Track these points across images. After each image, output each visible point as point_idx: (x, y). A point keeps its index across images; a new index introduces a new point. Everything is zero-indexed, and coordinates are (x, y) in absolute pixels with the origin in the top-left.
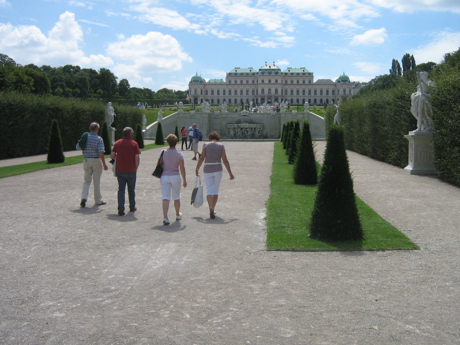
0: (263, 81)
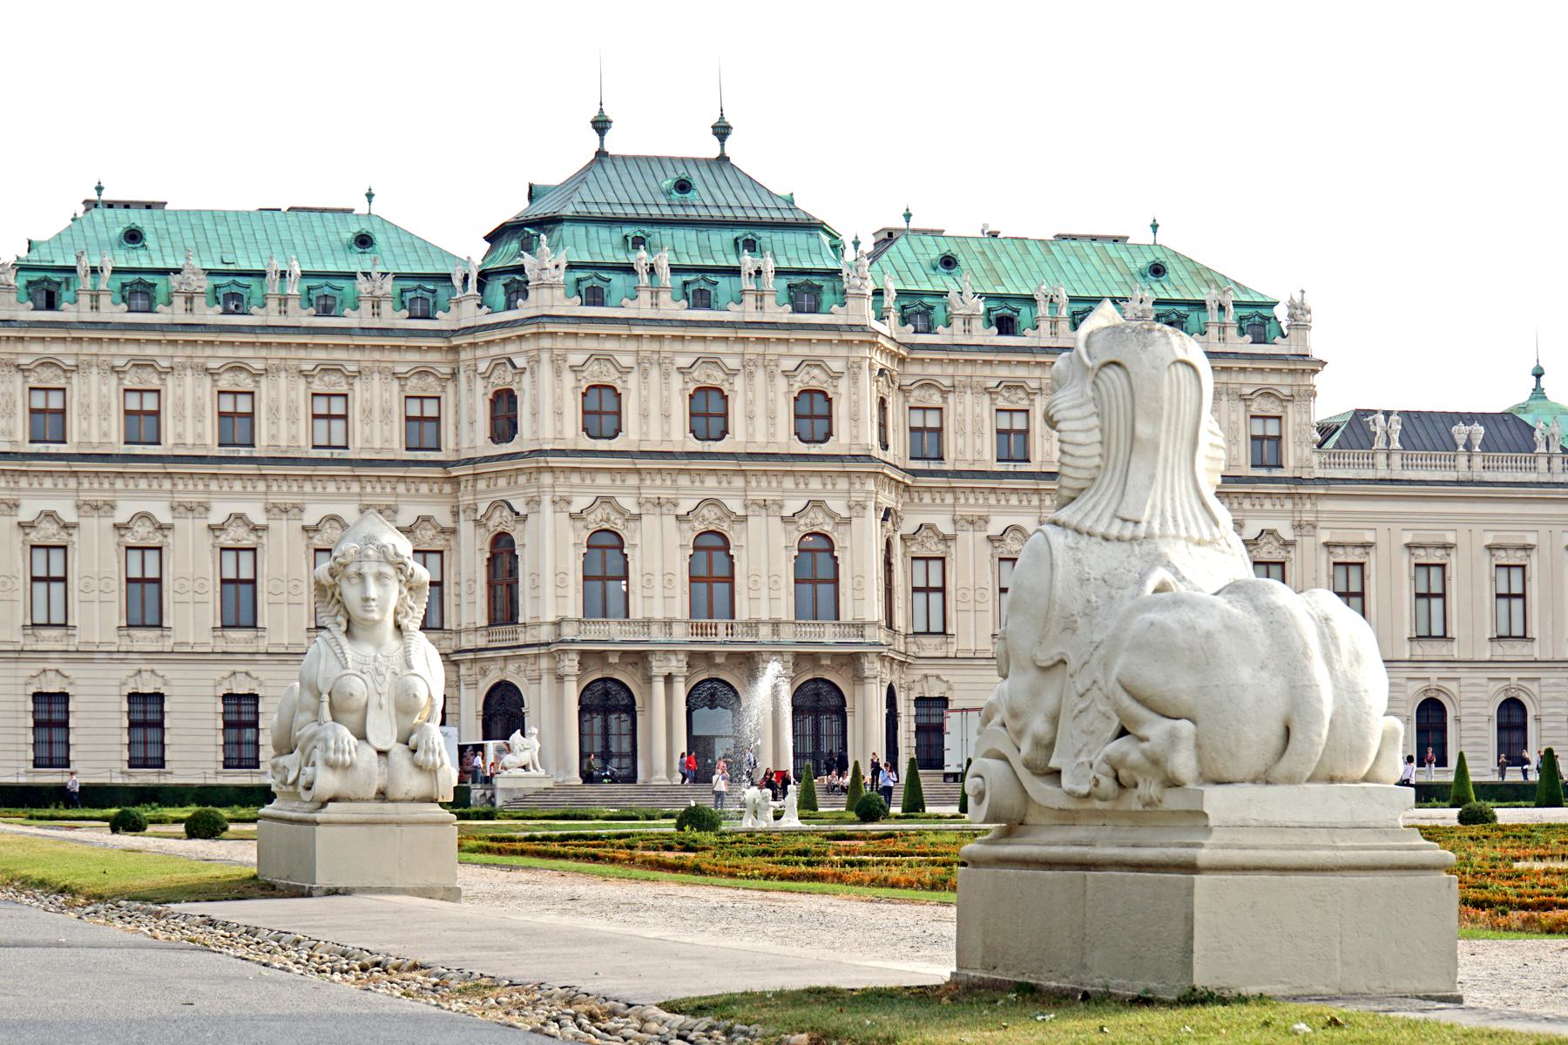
0: (602, 409)
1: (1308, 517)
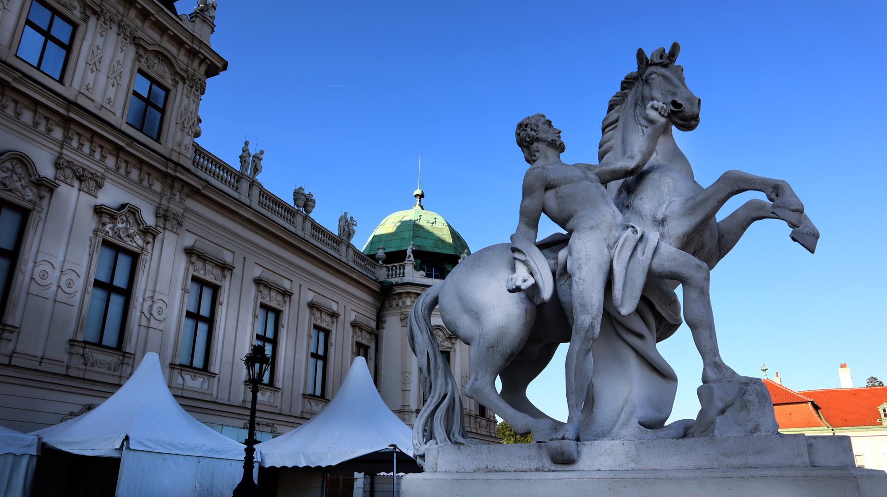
1: (175, 208)
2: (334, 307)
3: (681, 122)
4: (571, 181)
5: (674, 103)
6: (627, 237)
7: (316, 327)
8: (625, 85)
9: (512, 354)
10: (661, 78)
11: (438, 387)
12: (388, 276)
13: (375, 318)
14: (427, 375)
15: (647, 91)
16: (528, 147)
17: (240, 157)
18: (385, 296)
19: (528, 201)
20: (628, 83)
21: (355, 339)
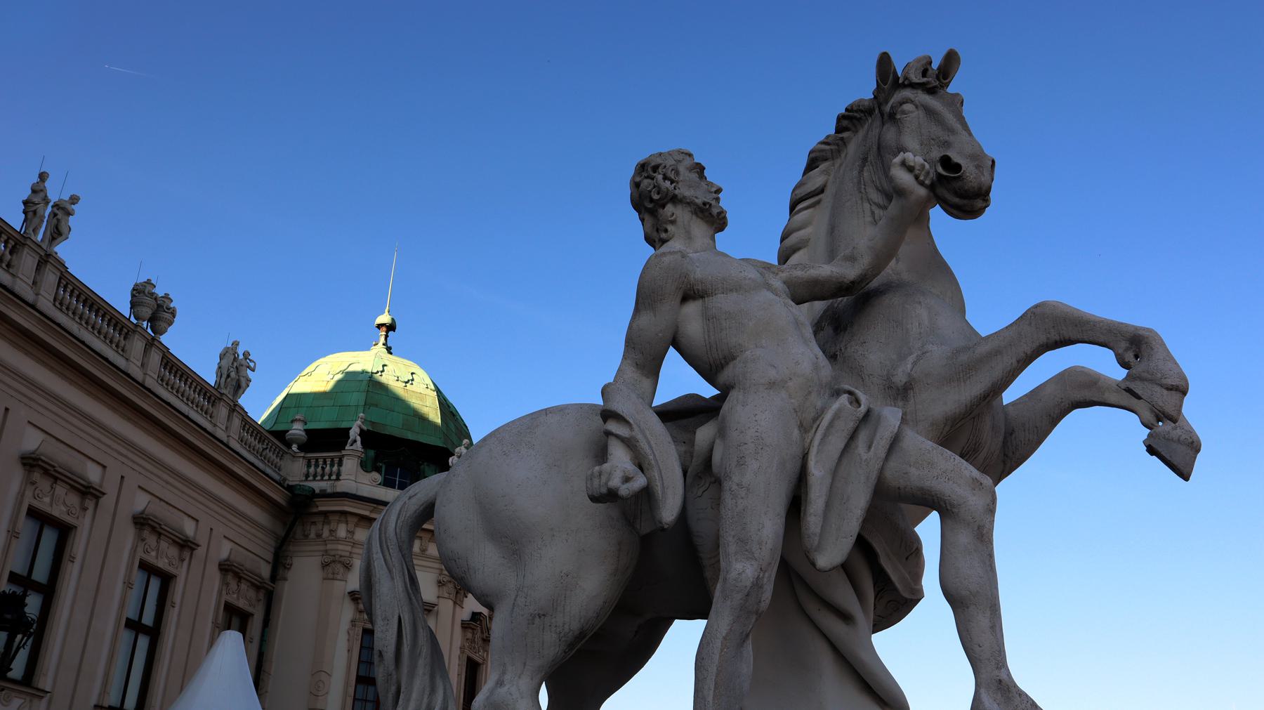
2: (189, 528)
3: (956, 200)
4: (736, 287)
5: (946, 162)
6: (839, 411)
7: (145, 567)
8: (845, 123)
9: (581, 635)
10: (921, 113)
11: (414, 696)
12: (307, 476)
13: (270, 557)
14: (392, 667)
15: (890, 134)
16: (653, 213)
17: (25, 203)
18: (296, 513)
19: (646, 319)
20: (850, 120)
21: (225, 597)
